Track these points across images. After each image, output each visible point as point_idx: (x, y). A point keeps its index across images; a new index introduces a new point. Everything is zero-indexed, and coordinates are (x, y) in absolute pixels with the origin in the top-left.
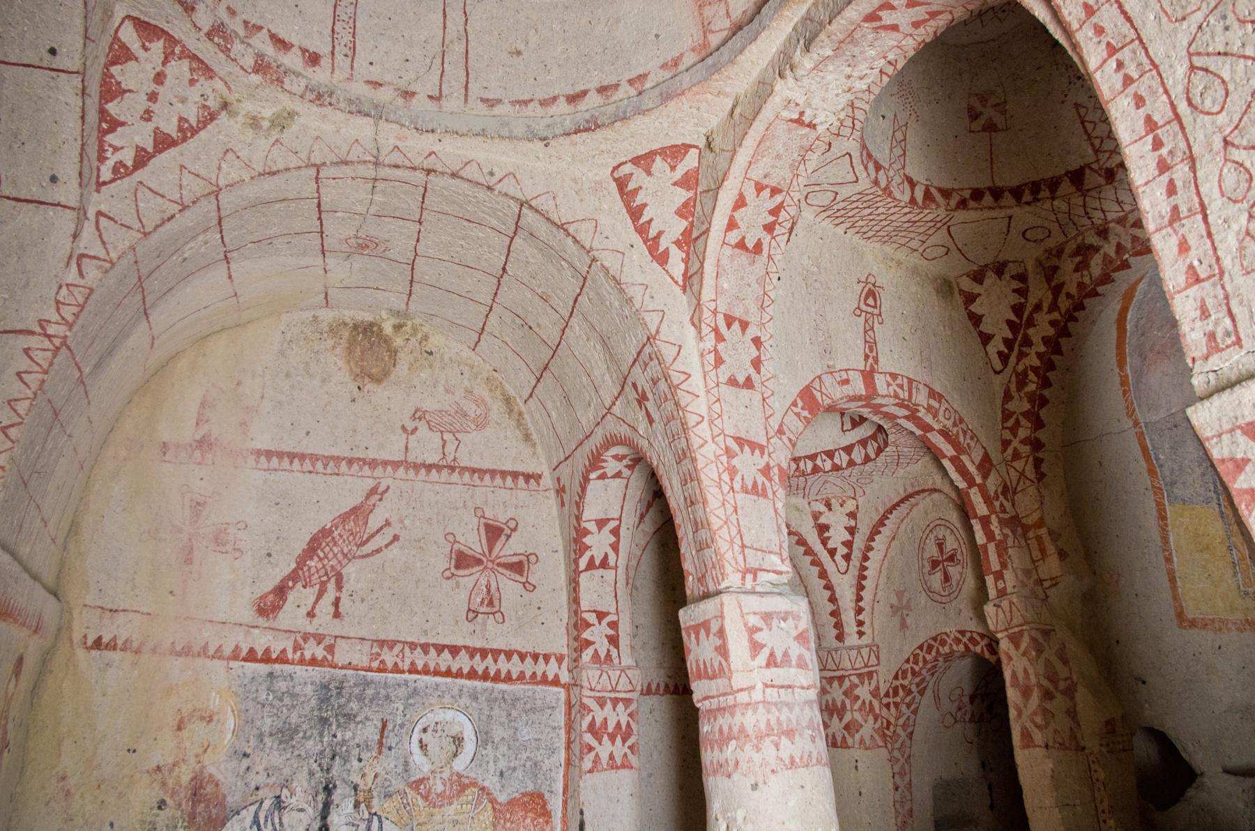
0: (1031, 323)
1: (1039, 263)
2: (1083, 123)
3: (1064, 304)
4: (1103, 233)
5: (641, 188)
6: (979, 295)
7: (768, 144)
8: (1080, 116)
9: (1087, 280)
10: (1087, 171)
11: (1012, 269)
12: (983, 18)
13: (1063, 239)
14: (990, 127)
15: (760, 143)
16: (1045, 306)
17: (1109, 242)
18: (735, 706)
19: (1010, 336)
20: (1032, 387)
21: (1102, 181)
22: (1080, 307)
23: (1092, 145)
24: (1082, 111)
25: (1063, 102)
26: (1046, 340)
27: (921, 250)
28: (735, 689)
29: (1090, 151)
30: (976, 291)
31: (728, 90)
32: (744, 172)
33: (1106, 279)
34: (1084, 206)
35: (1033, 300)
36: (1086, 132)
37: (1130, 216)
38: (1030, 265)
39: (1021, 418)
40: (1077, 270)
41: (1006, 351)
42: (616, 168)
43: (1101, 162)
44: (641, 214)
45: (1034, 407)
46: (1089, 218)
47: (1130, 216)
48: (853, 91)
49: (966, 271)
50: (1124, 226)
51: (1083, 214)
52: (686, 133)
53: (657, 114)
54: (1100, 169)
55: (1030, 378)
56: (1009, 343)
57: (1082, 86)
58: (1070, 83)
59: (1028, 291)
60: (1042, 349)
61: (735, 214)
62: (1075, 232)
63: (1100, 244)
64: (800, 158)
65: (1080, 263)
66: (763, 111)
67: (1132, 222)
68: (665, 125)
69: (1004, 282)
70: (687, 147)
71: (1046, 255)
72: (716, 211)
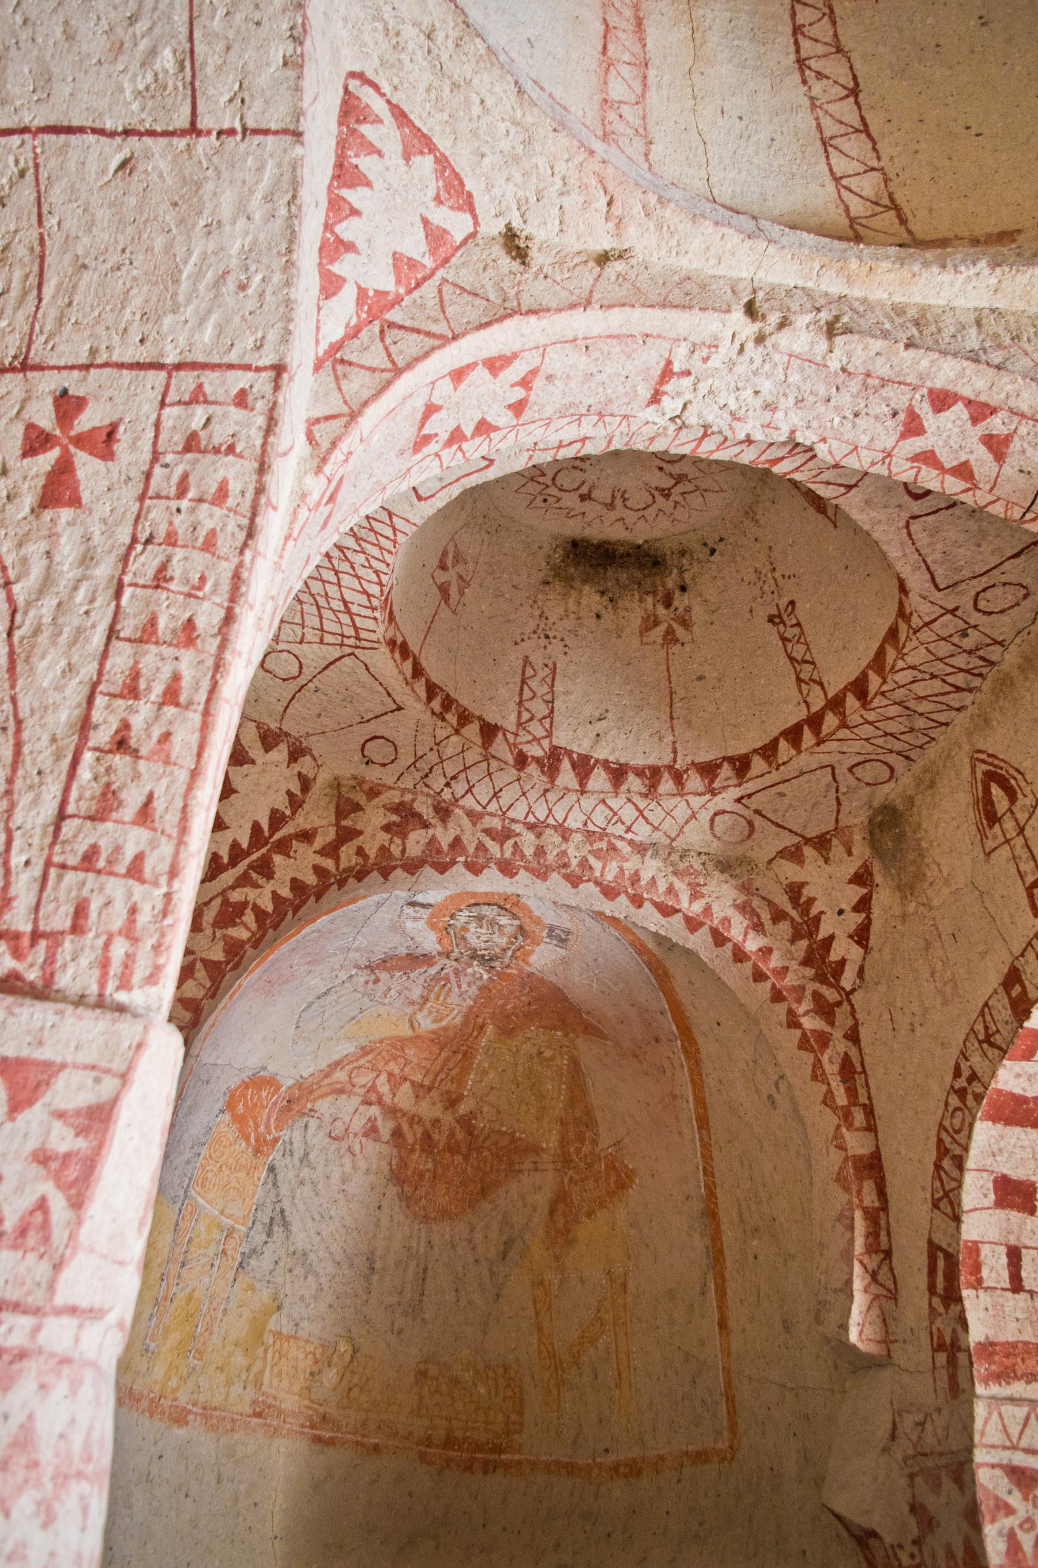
0: (283, 847)
1: (337, 784)
3: (348, 855)
4: (443, 812)
5: (380, 153)
6: (253, 762)
7: (617, 349)
8: (524, 673)
9: (396, 850)
10: (500, 735)
11: (305, 765)
12: (530, 484)
13: (390, 781)
14: (444, 590)
15: (617, 337)
16: (319, 842)
17: (445, 828)
18: (22, 1355)
19: (245, 845)
20: (240, 933)
21: (510, 760)
22: (361, 875)
23: (520, 713)
24: (529, 672)
25: (516, 643)
26: (296, 885)
27: (282, 646)
28: (60, 1299)
29: (513, 718)
30: (252, 754)
31: (632, 230)
33: (413, 867)
34: (466, 769)
35: (302, 821)
36: (521, 694)
37: (487, 818)
38: (324, 777)
39: (199, 965)
40: (387, 828)
41: (226, 860)
42: (360, 76)
43: (519, 739)
44: (352, 186)
45: (228, 963)
46: (448, 785)
47: (487, 818)
48: (735, 424)
49: (265, 719)
50: (474, 824)
51: (449, 775)
52: (497, 191)
53: (529, 119)
54: (515, 745)
55: (244, 918)
56: (237, 853)
57: (545, 648)
58: (535, 632)
59: (300, 806)
60: (285, 892)
61: (480, 366)
62: (411, 786)
63: (433, 821)
64: (584, 411)
65: (394, 823)
66: (686, 314)
67: (488, 826)
68: (504, 145)
69: (287, 773)
70: (468, 205)
71: (353, 783)
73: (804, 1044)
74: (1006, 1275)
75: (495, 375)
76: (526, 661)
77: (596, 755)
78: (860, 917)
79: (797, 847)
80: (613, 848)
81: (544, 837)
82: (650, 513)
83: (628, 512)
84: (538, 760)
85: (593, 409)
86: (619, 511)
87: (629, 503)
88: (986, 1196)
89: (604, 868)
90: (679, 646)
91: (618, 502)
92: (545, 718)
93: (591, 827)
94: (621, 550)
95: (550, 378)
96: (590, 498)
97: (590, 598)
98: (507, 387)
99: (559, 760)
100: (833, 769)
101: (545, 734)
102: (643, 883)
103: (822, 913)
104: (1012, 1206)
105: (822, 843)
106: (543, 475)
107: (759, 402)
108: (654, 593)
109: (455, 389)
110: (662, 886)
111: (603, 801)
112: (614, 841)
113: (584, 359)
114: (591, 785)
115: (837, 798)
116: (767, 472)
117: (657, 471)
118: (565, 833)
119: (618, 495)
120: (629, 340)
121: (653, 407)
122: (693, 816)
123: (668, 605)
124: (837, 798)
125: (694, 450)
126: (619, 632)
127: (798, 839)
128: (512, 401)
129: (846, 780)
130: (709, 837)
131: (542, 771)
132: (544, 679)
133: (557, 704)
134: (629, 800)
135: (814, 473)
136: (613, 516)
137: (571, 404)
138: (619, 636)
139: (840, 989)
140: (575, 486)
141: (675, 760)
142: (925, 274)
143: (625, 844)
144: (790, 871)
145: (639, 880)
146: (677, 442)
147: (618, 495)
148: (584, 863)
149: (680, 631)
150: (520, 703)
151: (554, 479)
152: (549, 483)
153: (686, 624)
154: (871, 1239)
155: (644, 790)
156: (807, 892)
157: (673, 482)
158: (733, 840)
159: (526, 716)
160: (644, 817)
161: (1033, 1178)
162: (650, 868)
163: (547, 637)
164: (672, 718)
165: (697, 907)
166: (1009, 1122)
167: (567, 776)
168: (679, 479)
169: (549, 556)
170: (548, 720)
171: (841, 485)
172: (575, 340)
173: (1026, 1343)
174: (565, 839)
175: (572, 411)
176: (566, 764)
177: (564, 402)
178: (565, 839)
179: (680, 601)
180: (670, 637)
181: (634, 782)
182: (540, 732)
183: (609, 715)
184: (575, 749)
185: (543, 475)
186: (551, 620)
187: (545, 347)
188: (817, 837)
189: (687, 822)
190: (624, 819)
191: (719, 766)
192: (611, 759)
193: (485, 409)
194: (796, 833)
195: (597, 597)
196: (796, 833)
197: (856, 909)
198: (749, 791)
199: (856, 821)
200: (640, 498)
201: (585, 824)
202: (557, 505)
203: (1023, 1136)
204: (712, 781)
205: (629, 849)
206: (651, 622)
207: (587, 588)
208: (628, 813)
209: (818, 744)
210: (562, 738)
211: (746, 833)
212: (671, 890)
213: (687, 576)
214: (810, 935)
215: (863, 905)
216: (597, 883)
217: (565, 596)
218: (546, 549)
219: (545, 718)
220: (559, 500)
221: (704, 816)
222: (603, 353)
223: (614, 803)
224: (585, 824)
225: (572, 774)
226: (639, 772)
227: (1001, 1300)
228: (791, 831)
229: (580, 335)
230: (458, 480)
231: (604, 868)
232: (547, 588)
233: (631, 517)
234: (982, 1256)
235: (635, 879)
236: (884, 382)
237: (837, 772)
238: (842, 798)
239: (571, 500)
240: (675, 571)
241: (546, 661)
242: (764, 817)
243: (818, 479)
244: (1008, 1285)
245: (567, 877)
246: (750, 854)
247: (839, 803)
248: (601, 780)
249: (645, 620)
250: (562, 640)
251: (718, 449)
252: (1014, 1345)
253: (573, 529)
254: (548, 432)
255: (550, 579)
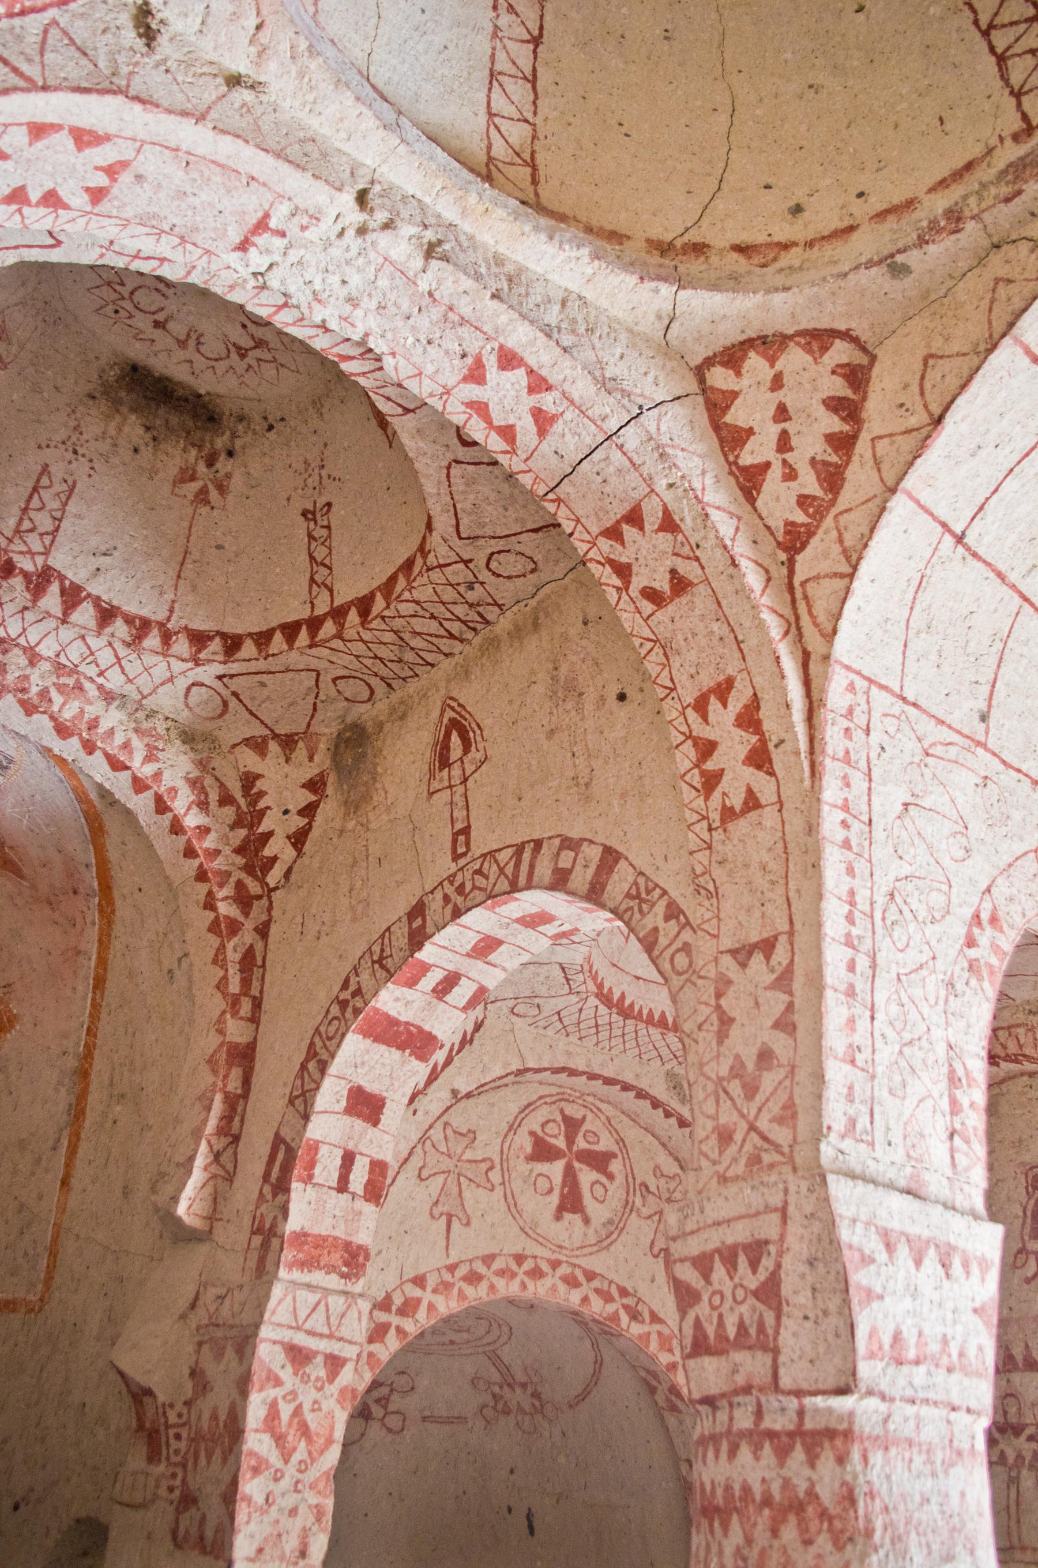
2: (35, 489)
7: (218, 179)
8: (38, 481)
12: (105, 288)
15: (222, 166)
23: (21, 520)
24: (45, 481)
25: (40, 447)
29: (12, 522)
31: (273, 66)
32: (155, 139)
43: (12, 547)
48: (315, 304)
57: (70, 462)
61: (66, 132)
66: (298, 174)
72: (78, 97)
73: (214, 927)
74: (336, 1175)
75: (80, 149)
76: (45, 469)
77: (89, 589)
78: (302, 822)
79: (265, 739)
80: (79, 687)
81: (10, 654)
82: (221, 366)
83: (199, 356)
84: (26, 575)
85: (177, 229)
86: (190, 352)
87: (202, 348)
88: (338, 1101)
89: (64, 704)
90: (208, 508)
91: (192, 343)
92: (47, 533)
93: (63, 660)
94: (180, 392)
95: (139, 177)
96: (164, 328)
97: (134, 429)
98: (89, 167)
99: (49, 582)
100: (318, 675)
101: (42, 550)
102: (101, 730)
103: (268, 808)
104: (359, 1115)
105: (288, 742)
106: (122, 284)
107: (343, 292)
108: (200, 448)
109: (31, 144)
110: (119, 739)
111: (83, 637)
112: (83, 680)
113: (181, 173)
114: (75, 617)
115: (315, 704)
116: (335, 364)
117: (239, 327)
118: (33, 657)
119: (194, 336)
120: (233, 175)
121: (238, 254)
122: (171, 679)
123: (210, 463)
124: (315, 704)
125: (270, 316)
126: (152, 473)
127: (268, 732)
128: (91, 185)
129: (327, 688)
130: (181, 705)
131: (28, 588)
132: (58, 494)
133: (64, 524)
134: (110, 644)
135: (379, 384)
136: (181, 354)
137: (155, 216)
138: (151, 478)
139: (263, 883)
140: (153, 309)
141: (169, 619)
142: (533, 238)
143: (94, 687)
144: (249, 760)
145: (96, 727)
146: (256, 301)
147: (194, 336)
148: (44, 694)
149: (214, 494)
150: (25, 510)
151: (132, 293)
152: (126, 295)
153: (222, 489)
154: (224, 1122)
155: (128, 639)
156: (259, 785)
157: (253, 344)
158: (204, 714)
159: (26, 525)
160: (121, 666)
161: (385, 1094)
162: (112, 718)
163: (75, 452)
164: (179, 577)
165: (147, 770)
166: (377, 1039)
167: (52, 600)
168: (260, 344)
169: (103, 371)
170: (50, 537)
171: (400, 405)
172: (177, 150)
173: (336, 1238)
174: (32, 664)
175: (154, 223)
176: (55, 588)
177: (148, 209)
178: (32, 664)
179: (223, 465)
180: (202, 497)
181: (120, 628)
182: (37, 546)
183: (116, 554)
184: (70, 575)
185: (122, 284)
186: (85, 437)
187: (143, 142)
188: (286, 735)
189: (162, 684)
190: (99, 661)
191: (211, 638)
192: (105, 597)
193: (59, 181)
194: (266, 726)
195: (141, 431)
196: (266, 726)
197: (301, 813)
198: (232, 672)
199: (326, 731)
200: (213, 346)
201: (58, 655)
202: (128, 321)
203: (386, 1054)
204: (199, 651)
205: (97, 693)
206: (187, 475)
207: (133, 417)
208: (105, 657)
209: (310, 647)
210: (58, 560)
211: (219, 711)
212: (126, 746)
213: (238, 443)
214: (251, 826)
215: (309, 811)
216: (52, 718)
217: (108, 417)
218: (103, 361)
219: (47, 533)
220: (131, 317)
221: (182, 683)
222: (202, 176)
223: (94, 642)
224: (58, 655)
225: (58, 600)
226: (129, 620)
227: (325, 1197)
228: (262, 722)
229: (184, 147)
230: (16, 247)
231: (64, 704)
232: (91, 402)
233: (200, 363)
234: (319, 1156)
235: (93, 725)
236: (463, 321)
237: (321, 678)
238: (319, 705)
239: (142, 322)
240: (228, 433)
241: (67, 477)
242: (241, 701)
243: (381, 391)
244: (335, 1185)
245: (23, 703)
246: (217, 733)
247: (315, 709)
248: (87, 616)
249: (183, 470)
250: (91, 461)
251: (294, 324)
252: (325, 1239)
253: (137, 352)
254: (123, 234)
255: (97, 395)
